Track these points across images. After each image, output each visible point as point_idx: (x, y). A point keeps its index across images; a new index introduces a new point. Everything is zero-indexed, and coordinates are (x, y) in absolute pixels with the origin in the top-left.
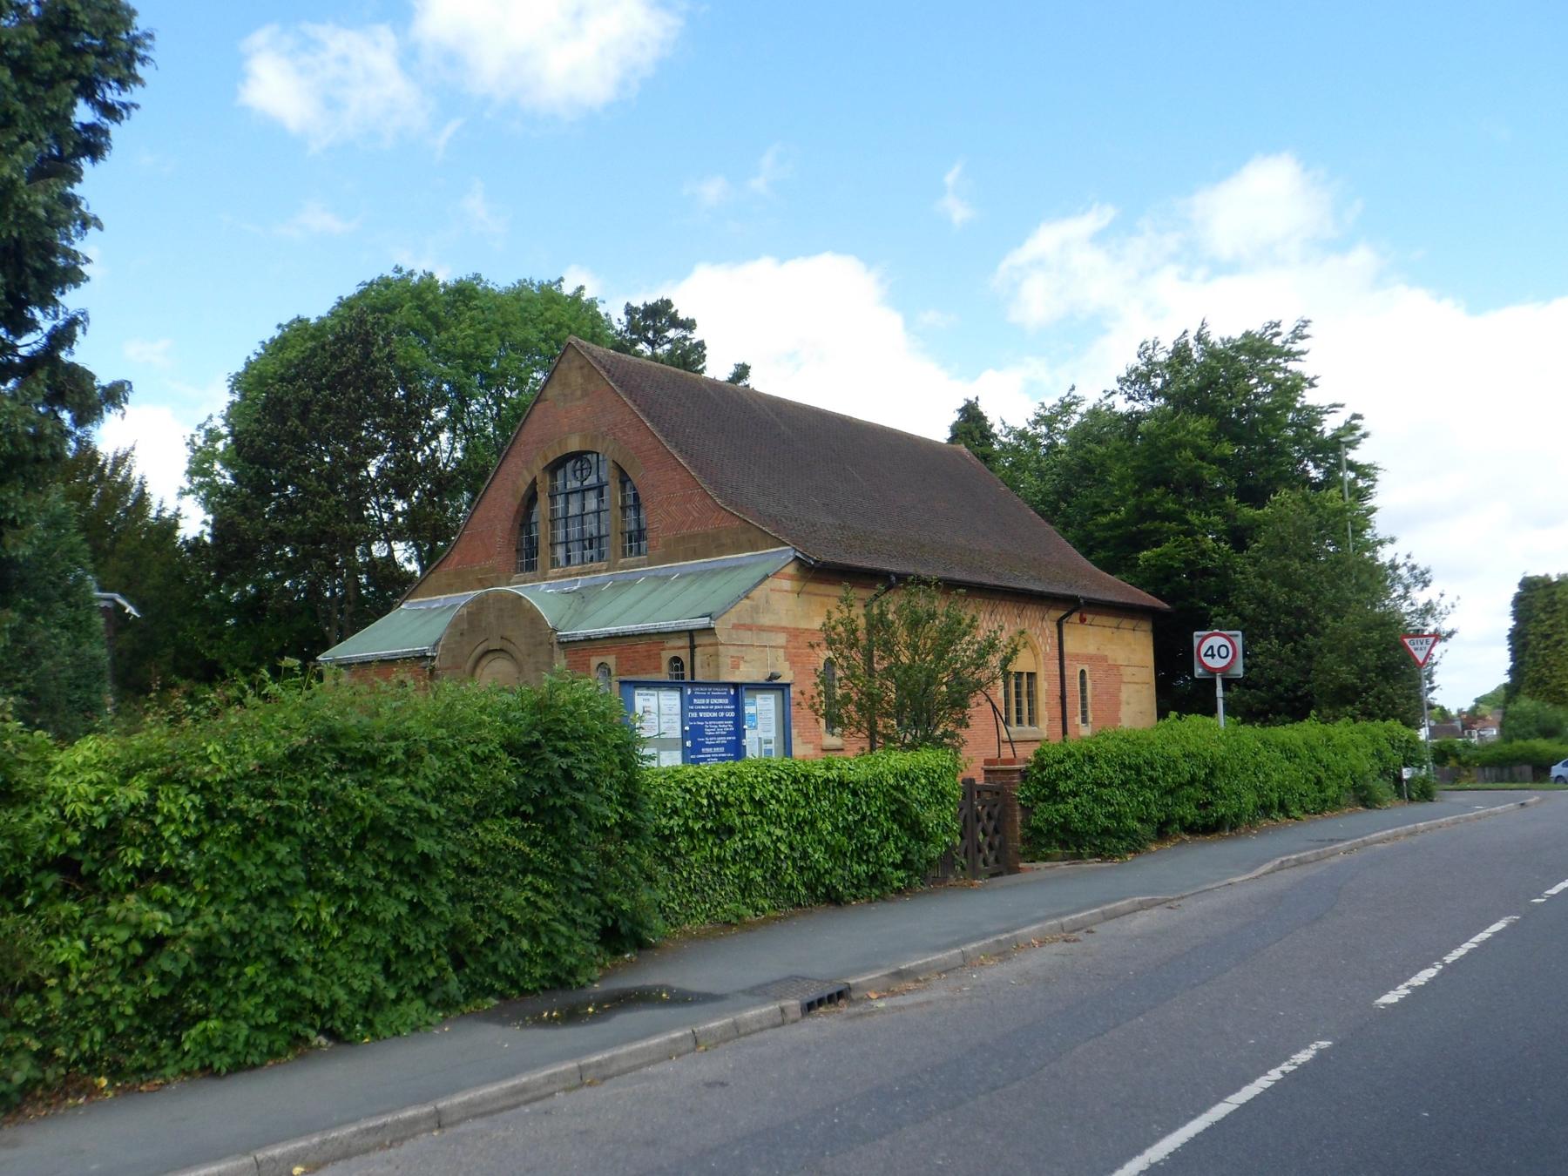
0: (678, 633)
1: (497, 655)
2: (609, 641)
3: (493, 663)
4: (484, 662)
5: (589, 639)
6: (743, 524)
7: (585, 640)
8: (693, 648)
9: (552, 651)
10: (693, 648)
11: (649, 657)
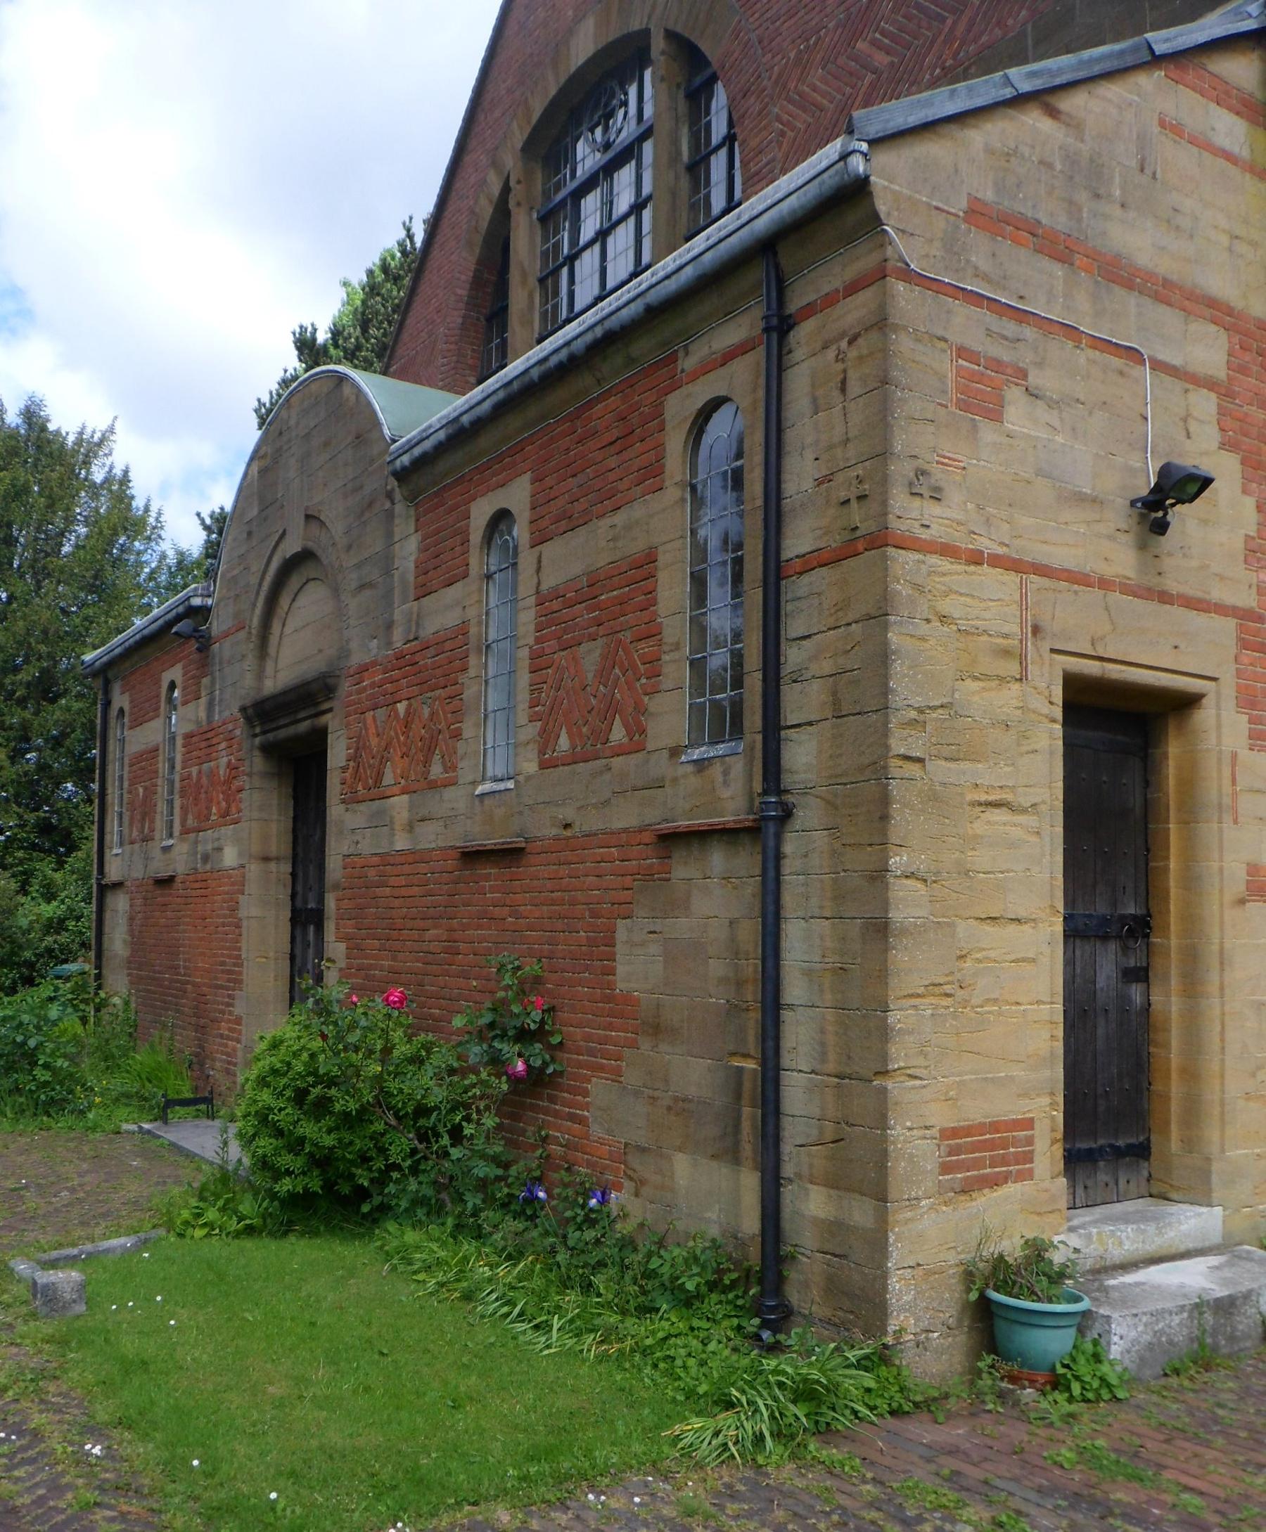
2: (513, 422)
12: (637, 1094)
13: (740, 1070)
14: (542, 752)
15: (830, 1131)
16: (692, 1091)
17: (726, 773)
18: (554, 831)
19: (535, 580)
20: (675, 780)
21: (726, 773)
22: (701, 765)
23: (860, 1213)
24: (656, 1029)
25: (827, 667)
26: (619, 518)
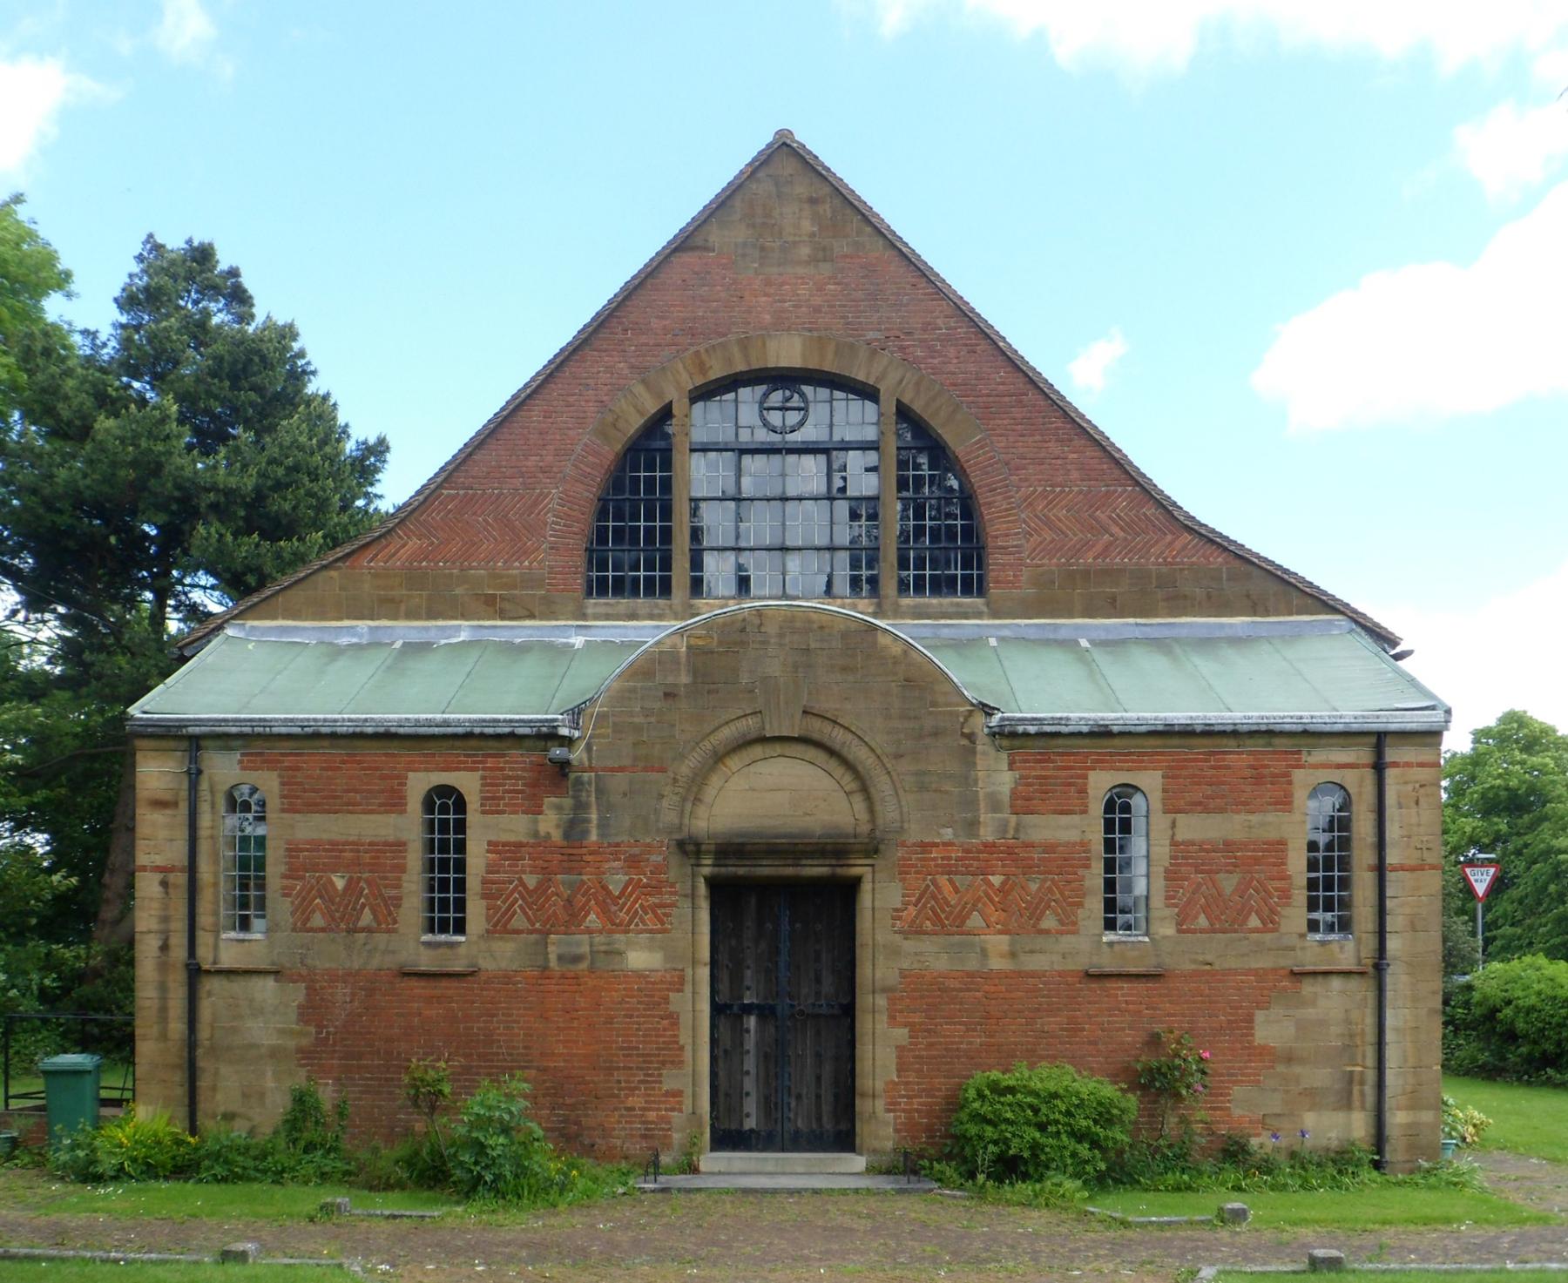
0: (1347, 736)
1: (778, 748)
2: (1152, 741)
4: (734, 763)
8: (1379, 767)
9: (968, 753)
10: (1379, 767)
11: (1258, 780)
12: (1274, 1090)
13: (1351, 1072)
14: (1179, 924)
16: (1318, 1084)
17: (1342, 948)
18: (1194, 967)
19: (1170, 832)
20: (1303, 949)
21: (1342, 948)
22: (1323, 943)
24: (1290, 1058)
25: (1408, 910)
26: (1254, 818)
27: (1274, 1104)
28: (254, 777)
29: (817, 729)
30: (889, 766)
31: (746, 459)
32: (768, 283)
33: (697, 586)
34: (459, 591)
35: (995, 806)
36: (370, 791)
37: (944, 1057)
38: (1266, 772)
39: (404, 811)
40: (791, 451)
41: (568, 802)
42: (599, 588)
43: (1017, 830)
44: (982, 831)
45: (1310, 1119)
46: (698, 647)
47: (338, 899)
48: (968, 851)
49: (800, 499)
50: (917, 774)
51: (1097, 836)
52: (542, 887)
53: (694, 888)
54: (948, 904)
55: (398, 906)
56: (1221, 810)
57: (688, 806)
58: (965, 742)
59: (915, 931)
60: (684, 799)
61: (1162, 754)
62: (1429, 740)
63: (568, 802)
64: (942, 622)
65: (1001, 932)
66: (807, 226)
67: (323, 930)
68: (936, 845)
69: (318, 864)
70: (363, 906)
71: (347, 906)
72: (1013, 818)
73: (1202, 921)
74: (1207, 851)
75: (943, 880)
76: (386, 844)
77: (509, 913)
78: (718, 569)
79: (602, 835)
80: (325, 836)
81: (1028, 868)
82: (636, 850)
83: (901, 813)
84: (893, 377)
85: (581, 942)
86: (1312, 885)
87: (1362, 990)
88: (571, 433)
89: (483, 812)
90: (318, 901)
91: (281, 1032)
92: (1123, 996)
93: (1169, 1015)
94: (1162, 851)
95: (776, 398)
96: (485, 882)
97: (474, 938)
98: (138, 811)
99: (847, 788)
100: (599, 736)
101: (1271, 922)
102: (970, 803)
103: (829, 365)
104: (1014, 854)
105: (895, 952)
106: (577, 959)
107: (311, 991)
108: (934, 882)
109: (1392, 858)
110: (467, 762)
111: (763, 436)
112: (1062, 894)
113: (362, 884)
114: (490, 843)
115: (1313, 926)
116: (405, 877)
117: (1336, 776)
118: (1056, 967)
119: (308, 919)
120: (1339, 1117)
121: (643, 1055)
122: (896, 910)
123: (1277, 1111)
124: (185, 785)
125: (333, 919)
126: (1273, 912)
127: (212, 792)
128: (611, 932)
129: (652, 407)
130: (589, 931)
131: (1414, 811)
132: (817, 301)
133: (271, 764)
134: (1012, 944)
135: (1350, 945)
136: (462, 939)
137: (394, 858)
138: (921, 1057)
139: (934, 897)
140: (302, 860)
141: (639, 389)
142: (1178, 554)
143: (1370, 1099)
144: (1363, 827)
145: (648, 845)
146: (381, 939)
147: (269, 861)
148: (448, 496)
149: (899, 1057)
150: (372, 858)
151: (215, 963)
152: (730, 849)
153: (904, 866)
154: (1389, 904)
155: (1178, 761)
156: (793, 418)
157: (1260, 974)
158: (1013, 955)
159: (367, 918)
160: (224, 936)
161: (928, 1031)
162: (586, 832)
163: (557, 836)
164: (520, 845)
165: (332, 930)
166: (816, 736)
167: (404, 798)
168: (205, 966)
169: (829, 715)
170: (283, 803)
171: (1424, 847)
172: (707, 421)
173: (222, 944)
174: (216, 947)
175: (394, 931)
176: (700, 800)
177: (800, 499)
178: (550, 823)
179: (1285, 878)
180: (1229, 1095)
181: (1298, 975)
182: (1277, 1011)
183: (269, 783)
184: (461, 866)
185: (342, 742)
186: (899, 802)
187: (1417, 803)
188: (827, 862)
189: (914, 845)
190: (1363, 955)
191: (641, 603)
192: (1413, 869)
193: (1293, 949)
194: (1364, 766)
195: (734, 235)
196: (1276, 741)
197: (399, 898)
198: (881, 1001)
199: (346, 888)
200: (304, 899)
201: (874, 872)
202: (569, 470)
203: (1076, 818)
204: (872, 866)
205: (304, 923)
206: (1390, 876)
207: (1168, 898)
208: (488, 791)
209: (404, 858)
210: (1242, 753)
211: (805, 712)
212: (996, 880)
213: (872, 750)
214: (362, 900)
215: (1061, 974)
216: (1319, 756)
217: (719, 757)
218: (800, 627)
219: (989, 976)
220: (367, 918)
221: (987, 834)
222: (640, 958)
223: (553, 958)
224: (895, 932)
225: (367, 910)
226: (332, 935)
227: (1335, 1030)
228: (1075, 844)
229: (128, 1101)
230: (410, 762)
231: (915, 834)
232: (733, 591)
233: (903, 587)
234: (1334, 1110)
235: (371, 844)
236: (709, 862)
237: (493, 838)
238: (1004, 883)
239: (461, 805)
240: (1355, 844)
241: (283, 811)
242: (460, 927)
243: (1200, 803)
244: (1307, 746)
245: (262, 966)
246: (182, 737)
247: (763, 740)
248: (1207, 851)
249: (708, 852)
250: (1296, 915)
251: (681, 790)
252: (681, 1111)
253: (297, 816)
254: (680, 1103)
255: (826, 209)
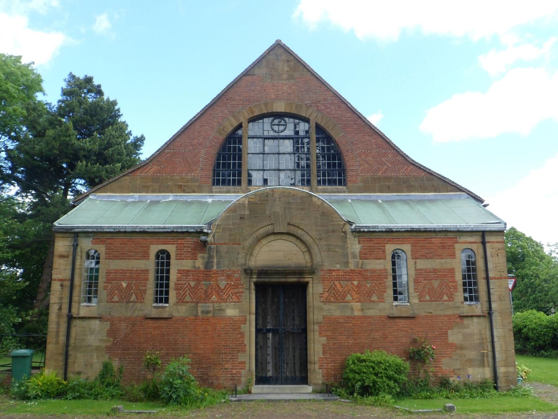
0: (472, 232)
1: (279, 237)
3: (273, 243)
4: (264, 242)
5: (390, 231)
6: (429, 175)
7: (386, 232)
8: (484, 243)
9: (345, 238)
10: (484, 243)
11: (444, 247)
12: (457, 360)
13: (483, 353)
14: (419, 298)
15: (504, 359)
16: (472, 357)
17: (476, 307)
18: (426, 314)
19: (414, 266)
22: (470, 305)
23: (511, 369)
24: (461, 348)
25: (498, 293)
26: (443, 261)
27: (457, 365)
28: (96, 247)
29: (292, 229)
30: (317, 243)
31: (266, 141)
32: (274, 86)
33: (250, 182)
34: (170, 183)
35: (354, 257)
36: (137, 252)
37: (339, 348)
38: (446, 244)
39: (149, 259)
40: (281, 138)
41: (206, 255)
42: (217, 182)
43: (362, 265)
44: (350, 265)
45: (470, 371)
46: (252, 202)
47: (123, 291)
48: (346, 273)
49: (284, 154)
50: (328, 245)
51: (389, 267)
52: (196, 286)
53: (250, 286)
54: (339, 291)
55: (145, 293)
56: (431, 258)
57: (248, 257)
58: (343, 234)
59: (327, 301)
60: (247, 255)
61: (410, 238)
62: (500, 234)
63: (206, 255)
64: (333, 194)
65: (357, 302)
66: (286, 68)
67: (117, 302)
68: (334, 270)
69: (117, 278)
70: (132, 293)
71: (127, 293)
72: (361, 261)
73: (428, 297)
74: (428, 272)
75: (337, 283)
76: (142, 270)
77: (184, 296)
78: (257, 177)
79: (218, 267)
80: (120, 268)
81: (366, 279)
82: (230, 273)
83: (322, 259)
84: (314, 115)
85: (210, 307)
86: (464, 284)
87: (484, 322)
88: (209, 132)
89: (177, 259)
90: (116, 291)
91: (101, 340)
92: (402, 325)
93: (418, 332)
94: (412, 272)
95: (276, 121)
96: (176, 284)
97: (171, 305)
98: (54, 259)
99: (303, 250)
100: (217, 232)
101: (451, 298)
102: (346, 255)
103: (293, 111)
104: (361, 274)
105: (321, 309)
106: (208, 312)
107: (112, 325)
108: (334, 283)
109: (491, 275)
110: (171, 241)
111: (272, 133)
112: (378, 287)
113: (133, 285)
114: (178, 270)
115: (466, 299)
116: (148, 282)
117: (469, 246)
118: (378, 314)
119: (112, 298)
120: (480, 370)
121: (231, 348)
122: (321, 294)
123: (458, 367)
124: (72, 250)
125: (122, 298)
126: (451, 294)
127: (81, 252)
128: (221, 302)
129: (236, 124)
130: (213, 302)
131: (497, 258)
132: (289, 91)
133: (102, 242)
134: (362, 306)
135: (479, 306)
136: (167, 305)
137: (145, 276)
138: (331, 348)
139: (334, 289)
140: (112, 277)
141: (232, 119)
142: (409, 172)
143: (491, 363)
144: (480, 264)
145: (234, 271)
146: (138, 305)
147: (100, 277)
148: (167, 152)
149: (323, 348)
150: (136, 276)
151: (78, 314)
152: (263, 272)
153: (324, 278)
154: (491, 291)
155: (416, 241)
156: (282, 128)
157: (449, 317)
158: (362, 310)
159: (133, 298)
160: (82, 304)
161: (334, 338)
162: (212, 266)
163: (202, 268)
164: (188, 271)
165: (121, 302)
166: (292, 232)
167: (149, 254)
168: (74, 316)
169: (296, 225)
170: (106, 256)
171: (501, 271)
172: (254, 129)
173: (81, 308)
174: (79, 309)
175: (143, 302)
176: (252, 255)
177: (284, 154)
178: (200, 263)
179: (454, 281)
180: (441, 362)
181: (462, 317)
182: (456, 330)
183: (102, 249)
184: (168, 278)
185: (128, 235)
186: (321, 255)
187: (498, 255)
188: (297, 277)
189: (327, 270)
190: (484, 309)
191: (231, 188)
192: (498, 279)
193: (459, 307)
194: (479, 243)
195: (261, 71)
196: (448, 234)
197: (145, 290)
198: (316, 327)
199: (127, 287)
200: (111, 291)
201: (313, 280)
202: (208, 144)
203: (382, 261)
204: (312, 278)
205: (111, 300)
206: (491, 281)
207: (415, 289)
208: (178, 252)
209: (148, 276)
210: (437, 238)
211: (288, 224)
212: (356, 283)
213: (311, 237)
214: (132, 291)
215: (380, 317)
216: (463, 239)
217: (259, 240)
218: (285, 194)
219: (354, 318)
220: (133, 298)
221: (352, 266)
222: (231, 312)
223: (199, 312)
224: (321, 302)
225: (134, 295)
226: (121, 304)
227: (476, 337)
228: (382, 270)
229: (42, 367)
230: (151, 241)
231: (327, 266)
232: (262, 184)
233: (319, 182)
234: (478, 367)
235: (136, 270)
236: (255, 277)
237: (180, 268)
238: (358, 284)
239: (168, 257)
240: (478, 269)
241: (106, 259)
242: (167, 301)
243: (424, 256)
244: (458, 236)
245: (95, 316)
246: (72, 233)
247: (274, 234)
248: (428, 272)
249: (255, 273)
250: (460, 295)
251: (246, 251)
252: (245, 369)
253: (110, 261)
254: (245, 366)
255: (292, 63)
